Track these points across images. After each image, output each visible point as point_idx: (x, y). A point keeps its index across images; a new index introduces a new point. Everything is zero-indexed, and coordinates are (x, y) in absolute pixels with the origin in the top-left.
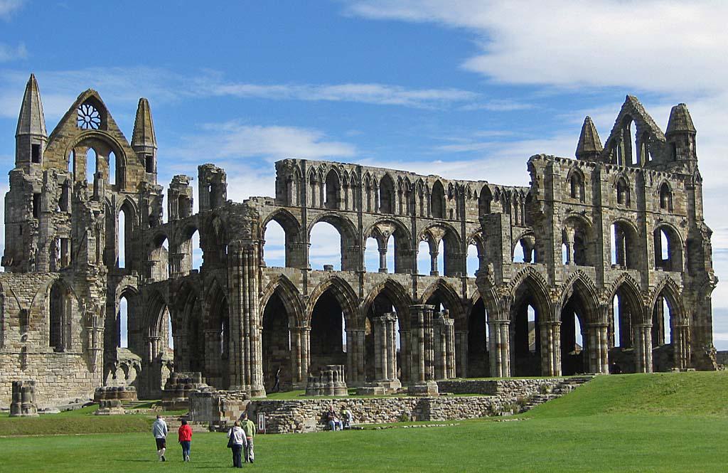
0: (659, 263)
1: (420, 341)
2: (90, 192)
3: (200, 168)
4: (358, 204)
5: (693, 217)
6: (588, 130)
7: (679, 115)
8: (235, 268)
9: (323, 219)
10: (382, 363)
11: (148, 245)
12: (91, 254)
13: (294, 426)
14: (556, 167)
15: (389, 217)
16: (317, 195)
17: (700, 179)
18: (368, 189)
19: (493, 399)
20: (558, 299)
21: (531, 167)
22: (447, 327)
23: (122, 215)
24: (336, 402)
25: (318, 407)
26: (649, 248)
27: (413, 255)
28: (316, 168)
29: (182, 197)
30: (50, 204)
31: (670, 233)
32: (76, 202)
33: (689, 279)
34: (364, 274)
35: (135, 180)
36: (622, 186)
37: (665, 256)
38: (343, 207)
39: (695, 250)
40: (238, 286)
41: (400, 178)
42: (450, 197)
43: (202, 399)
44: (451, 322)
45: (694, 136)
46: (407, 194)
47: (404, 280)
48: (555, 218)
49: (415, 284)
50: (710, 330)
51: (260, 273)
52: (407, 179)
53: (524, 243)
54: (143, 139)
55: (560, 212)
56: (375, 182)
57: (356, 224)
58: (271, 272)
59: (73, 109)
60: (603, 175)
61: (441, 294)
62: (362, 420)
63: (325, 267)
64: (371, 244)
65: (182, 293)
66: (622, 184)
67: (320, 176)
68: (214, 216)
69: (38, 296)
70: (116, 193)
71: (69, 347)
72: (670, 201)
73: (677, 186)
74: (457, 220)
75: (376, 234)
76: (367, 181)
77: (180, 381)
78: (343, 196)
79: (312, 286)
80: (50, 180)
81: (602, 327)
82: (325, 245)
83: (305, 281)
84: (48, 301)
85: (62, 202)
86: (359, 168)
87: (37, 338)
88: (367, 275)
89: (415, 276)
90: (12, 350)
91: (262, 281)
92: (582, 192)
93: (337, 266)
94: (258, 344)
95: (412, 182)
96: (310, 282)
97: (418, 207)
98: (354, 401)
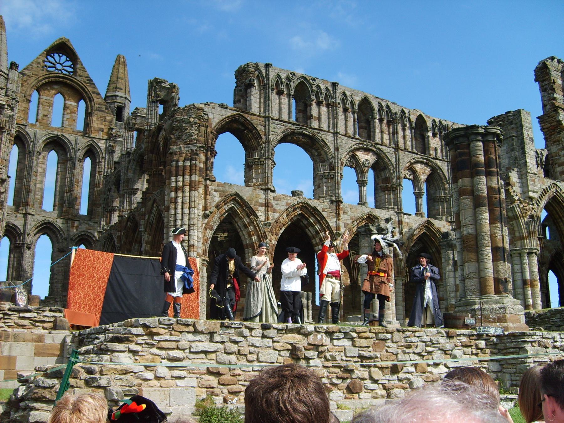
8: (173, 179)
15: (369, 144)
16: (283, 108)
18: (345, 110)
23: (88, 162)
24: (271, 333)
25: (210, 347)
27: (395, 189)
28: (283, 76)
34: (341, 205)
35: (102, 126)
38: (315, 124)
42: (434, 135)
46: (389, 123)
51: (206, 187)
52: (388, 107)
56: (352, 103)
58: (221, 189)
63: (294, 193)
67: (288, 86)
70: (80, 138)
74: (442, 160)
76: (344, 101)
79: (275, 211)
88: (344, 205)
91: (208, 197)
95: (394, 111)
96: (272, 207)
98: (329, 334)
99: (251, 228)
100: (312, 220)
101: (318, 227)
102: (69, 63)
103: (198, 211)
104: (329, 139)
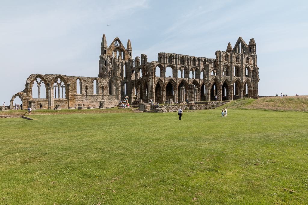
0: (246, 76)
1: (190, 92)
2: (117, 60)
3: (141, 55)
4: (176, 62)
5: (254, 65)
6: (229, 45)
7: (252, 41)
9: (169, 66)
10: (181, 98)
11: (130, 72)
12: (118, 74)
13: (162, 111)
14: (222, 53)
16: (167, 61)
17: (256, 56)
18: (179, 59)
19: (207, 106)
20: (222, 84)
21: (216, 54)
22: (196, 90)
23: (125, 66)
26: (243, 72)
28: (167, 54)
29: (138, 62)
30: (108, 63)
31: (248, 68)
32: (114, 62)
33: (253, 79)
36: (237, 58)
37: (247, 74)
38: (173, 63)
39: (255, 72)
40: (150, 81)
41: (186, 57)
42: (197, 61)
43: (142, 105)
44: (197, 89)
45: (255, 46)
46: (187, 60)
47: (186, 80)
48: (221, 65)
49: (189, 80)
50: (257, 91)
51: (155, 78)
53: (213, 72)
54: (129, 49)
55: (223, 64)
56: (180, 58)
57: (176, 67)
59: (113, 42)
60: (233, 55)
61: (195, 82)
62: (177, 110)
64: (179, 72)
65: (138, 82)
66: (237, 57)
67: (168, 56)
68: (145, 65)
69: (106, 83)
70: (123, 61)
71: (113, 94)
72: (249, 61)
73: (251, 58)
75: (180, 69)
76: (179, 57)
77: (137, 101)
78: (173, 61)
80: (108, 58)
81: (232, 90)
82: (169, 72)
83: (165, 80)
84: (108, 84)
85: (111, 62)
86: (177, 54)
87: (106, 92)
89: (189, 79)
90: (101, 95)
92: (228, 59)
93: (172, 77)
94: (154, 93)
97: (190, 63)
99: (162, 84)
100: (172, 81)
101: (173, 83)
102: (119, 45)
103: (154, 82)
104: (175, 66)
